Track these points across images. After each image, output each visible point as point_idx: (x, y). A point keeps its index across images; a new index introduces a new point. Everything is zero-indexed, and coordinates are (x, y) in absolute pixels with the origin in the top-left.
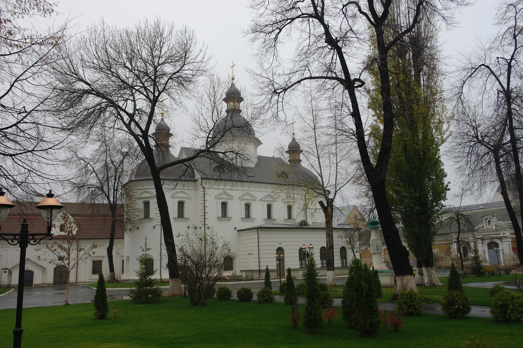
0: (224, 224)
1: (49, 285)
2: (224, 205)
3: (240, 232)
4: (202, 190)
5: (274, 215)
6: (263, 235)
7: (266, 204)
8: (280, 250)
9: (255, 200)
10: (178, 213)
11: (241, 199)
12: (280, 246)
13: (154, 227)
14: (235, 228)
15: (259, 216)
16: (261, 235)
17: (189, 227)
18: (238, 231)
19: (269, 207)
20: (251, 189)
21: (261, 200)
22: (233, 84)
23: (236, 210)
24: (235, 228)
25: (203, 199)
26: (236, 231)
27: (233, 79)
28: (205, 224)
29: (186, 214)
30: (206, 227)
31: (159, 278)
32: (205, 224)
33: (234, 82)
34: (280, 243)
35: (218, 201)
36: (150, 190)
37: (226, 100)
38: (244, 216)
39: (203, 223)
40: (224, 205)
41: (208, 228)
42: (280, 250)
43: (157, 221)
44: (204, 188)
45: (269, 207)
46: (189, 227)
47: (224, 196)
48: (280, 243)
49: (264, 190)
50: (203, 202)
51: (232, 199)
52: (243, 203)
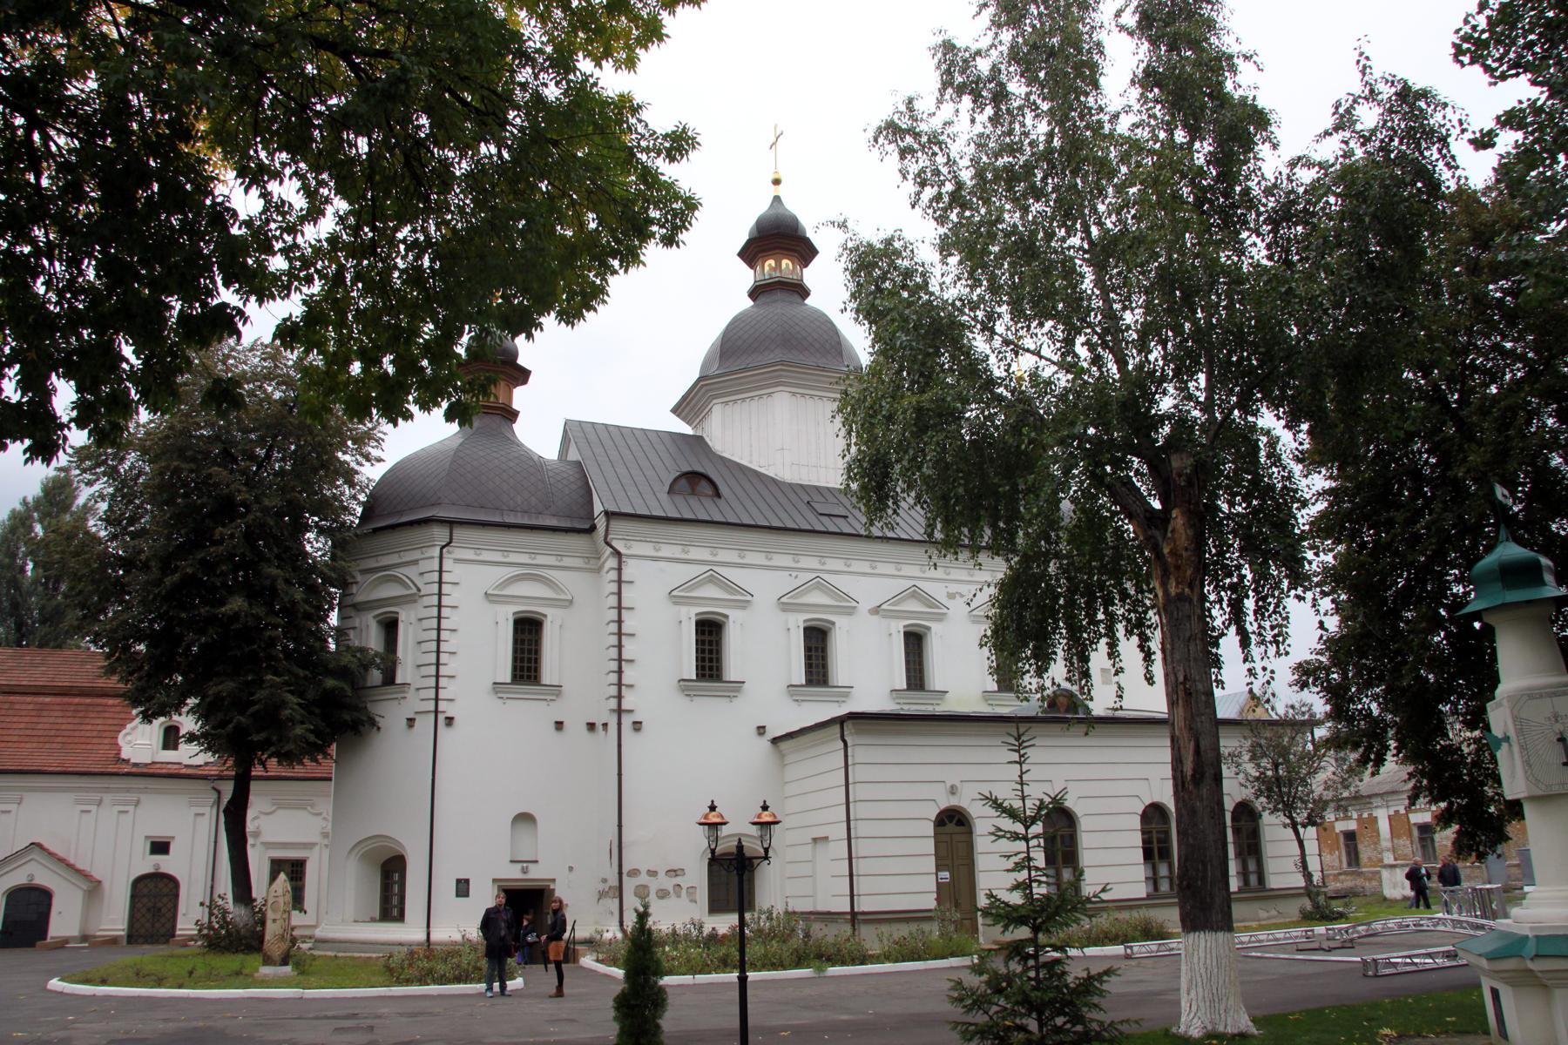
0: (710, 708)
1: (113, 941)
2: (710, 633)
3: (784, 745)
4: (612, 563)
5: (939, 672)
6: (869, 753)
7: (898, 628)
8: (953, 823)
9: (849, 611)
10: (515, 668)
11: (785, 606)
12: (953, 802)
13: (411, 722)
14: (761, 730)
15: (868, 673)
16: (857, 754)
17: (559, 725)
18: (775, 741)
19: (915, 642)
20: (833, 564)
21: (876, 610)
22: (777, 199)
23: (763, 650)
24: (761, 730)
25: (613, 601)
26: (764, 743)
27: (777, 182)
28: (619, 711)
29: (551, 665)
30: (627, 721)
31: (420, 936)
32: (619, 711)
33: (781, 191)
34: (953, 790)
35: (684, 609)
36: (402, 570)
37: (751, 253)
38: (799, 676)
39: (613, 704)
40: (710, 633)
41: (637, 726)
42: (953, 823)
43: (424, 694)
44: (618, 554)
45: (915, 642)
46: (559, 725)
47: (711, 591)
48: (953, 790)
49: (889, 569)
50: (613, 614)
51: (744, 605)
52: (798, 622)
